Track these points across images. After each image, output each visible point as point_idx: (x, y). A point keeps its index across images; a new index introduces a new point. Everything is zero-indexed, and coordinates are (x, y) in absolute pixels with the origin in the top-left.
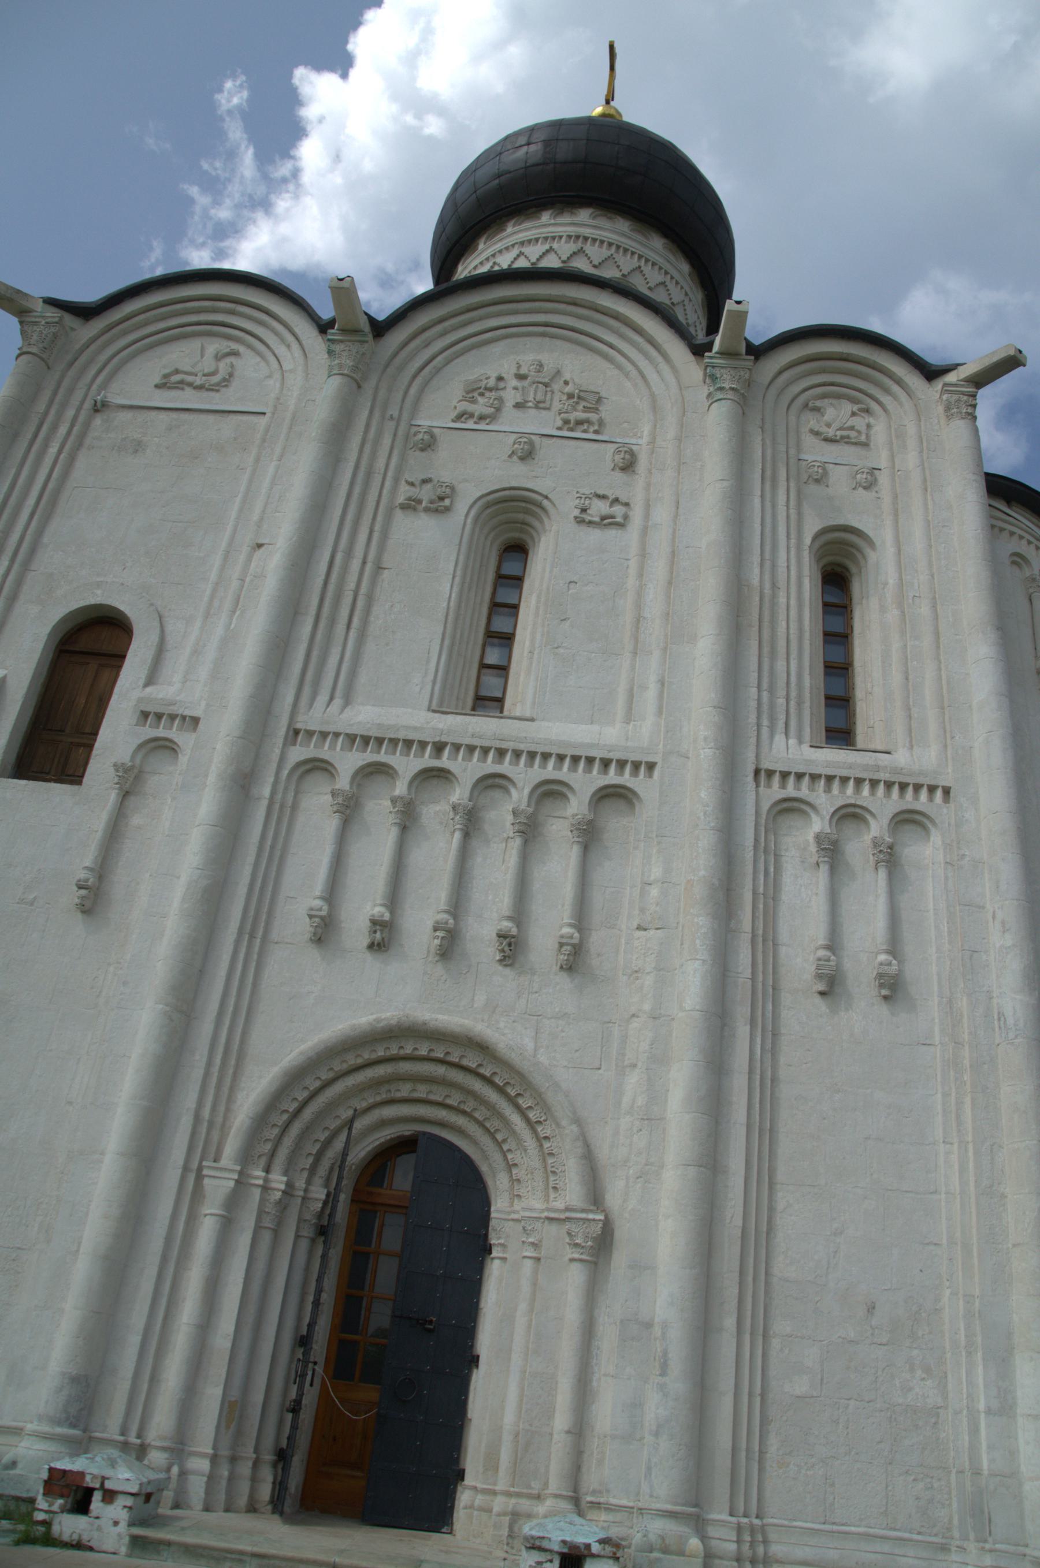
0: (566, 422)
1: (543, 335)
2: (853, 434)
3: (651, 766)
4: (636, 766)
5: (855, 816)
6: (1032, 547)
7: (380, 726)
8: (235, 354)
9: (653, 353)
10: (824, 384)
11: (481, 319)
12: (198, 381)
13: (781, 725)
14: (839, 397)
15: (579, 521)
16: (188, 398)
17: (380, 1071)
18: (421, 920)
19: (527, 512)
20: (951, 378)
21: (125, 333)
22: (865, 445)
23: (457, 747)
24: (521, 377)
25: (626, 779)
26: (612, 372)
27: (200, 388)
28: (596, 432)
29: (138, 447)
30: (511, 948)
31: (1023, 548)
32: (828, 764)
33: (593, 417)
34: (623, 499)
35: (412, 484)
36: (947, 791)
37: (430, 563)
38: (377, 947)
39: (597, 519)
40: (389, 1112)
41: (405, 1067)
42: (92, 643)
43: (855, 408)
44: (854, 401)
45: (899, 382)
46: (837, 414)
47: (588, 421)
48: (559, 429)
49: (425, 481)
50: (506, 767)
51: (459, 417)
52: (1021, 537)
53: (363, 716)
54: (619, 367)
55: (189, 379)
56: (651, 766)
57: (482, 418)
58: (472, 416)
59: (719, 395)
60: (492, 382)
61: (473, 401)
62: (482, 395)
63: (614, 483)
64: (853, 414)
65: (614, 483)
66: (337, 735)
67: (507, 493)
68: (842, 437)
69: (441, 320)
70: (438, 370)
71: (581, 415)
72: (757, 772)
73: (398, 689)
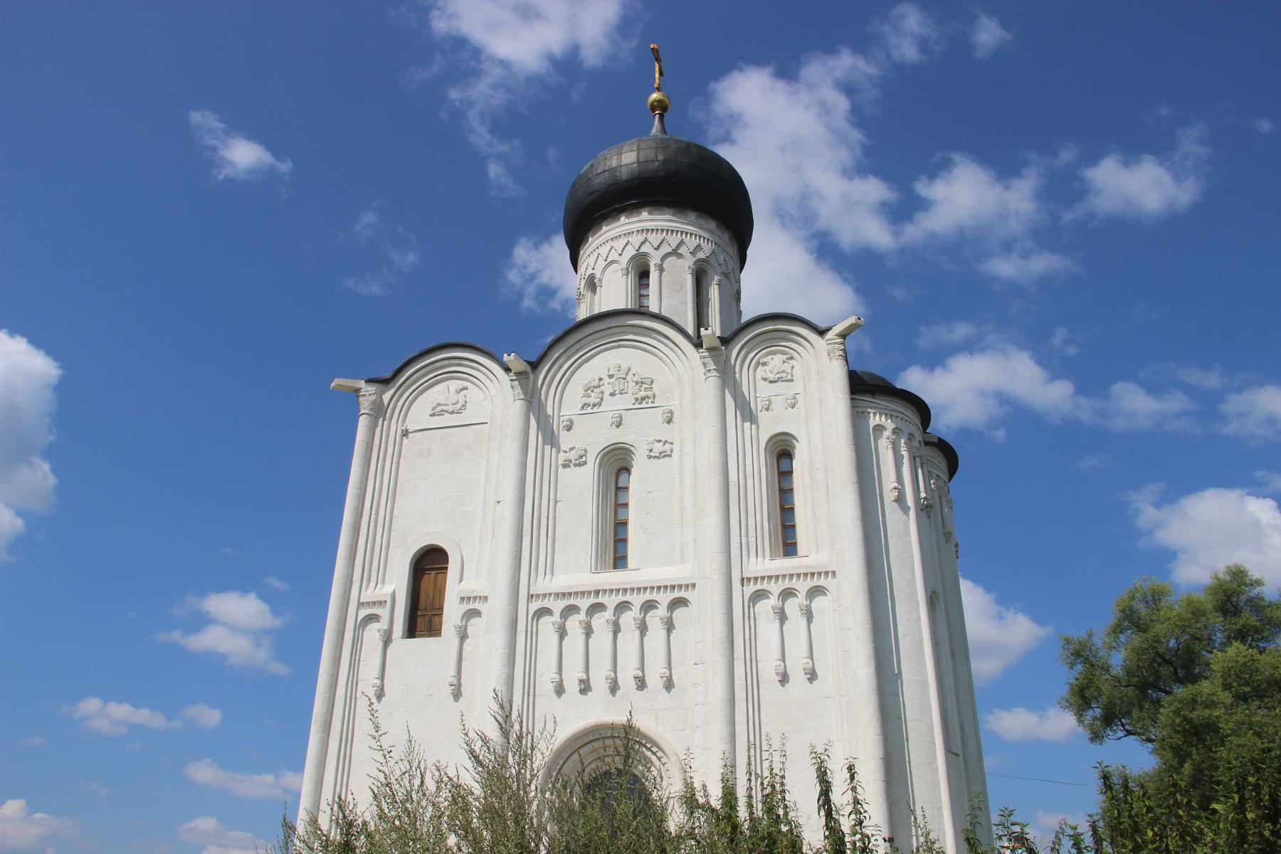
0: (637, 399)
1: (619, 347)
3: (694, 585)
4: (687, 586)
12: (450, 408)
15: (650, 457)
18: (599, 679)
21: (408, 388)
22: (792, 380)
24: (611, 376)
25: (683, 594)
27: (452, 413)
30: (641, 683)
36: (834, 573)
37: (580, 489)
42: (430, 562)
44: (784, 353)
46: (776, 362)
47: (648, 397)
50: (628, 598)
53: (561, 581)
55: (446, 408)
56: (694, 585)
57: (594, 405)
60: (596, 383)
63: (664, 432)
65: (664, 432)
71: (643, 394)
72: (743, 579)
73: (575, 567)
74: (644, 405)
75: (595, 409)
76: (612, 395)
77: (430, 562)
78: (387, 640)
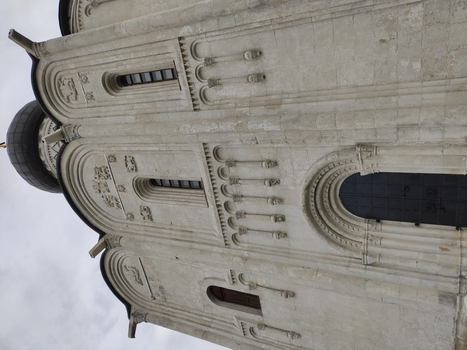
2: (71, 84)
4: (205, 149)
5: (200, 73)
6: (81, 5)
7: (217, 223)
8: (125, 266)
9: (74, 155)
10: (58, 97)
11: (87, 205)
13: (177, 102)
14: (60, 91)
15: (136, 170)
16: (142, 276)
17: (322, 213)
19: (140, 183)
20: (34, 54)
21: (130, 295)
22: (72, 79)
23: (217, 201)
24: (100, 191)
26: (86, 165)
28: (107, 168)
29: (161, 288)
31: (83, 10)
32: (185, 85)
33: (103, 169)
34: (124, 158)
35: (144, 218)
36: (180, 38)
38: (283, 219)
39: (134, 165)
40: (334, 206)
41: (319, 207)
43: (61, 84)
44: (59, 86)
45: (45, 71)
47: (105, 170)
48: (111, 179)
49: (142, 215)
51: (119, 207)
52: (79, 11)
54: (84, 163)
55: (137, 277)
56: (204, 144)
57: (117, 200)
58: (117, 204)
59: (77, 135)
60: (105, 199)
61: (113, 204)
62: (110, 201)
64: (64, 85)
66: (223, 234)
67: (136, 191)
68: (73, 88)
69: (92, 216)
70: (108, 214)
71: (104, 173)
72: (195, 110)
74: (110, 173)
75: (119, 200)
76: (109, 191)
77: (217, 294)
78: (262, 326)
